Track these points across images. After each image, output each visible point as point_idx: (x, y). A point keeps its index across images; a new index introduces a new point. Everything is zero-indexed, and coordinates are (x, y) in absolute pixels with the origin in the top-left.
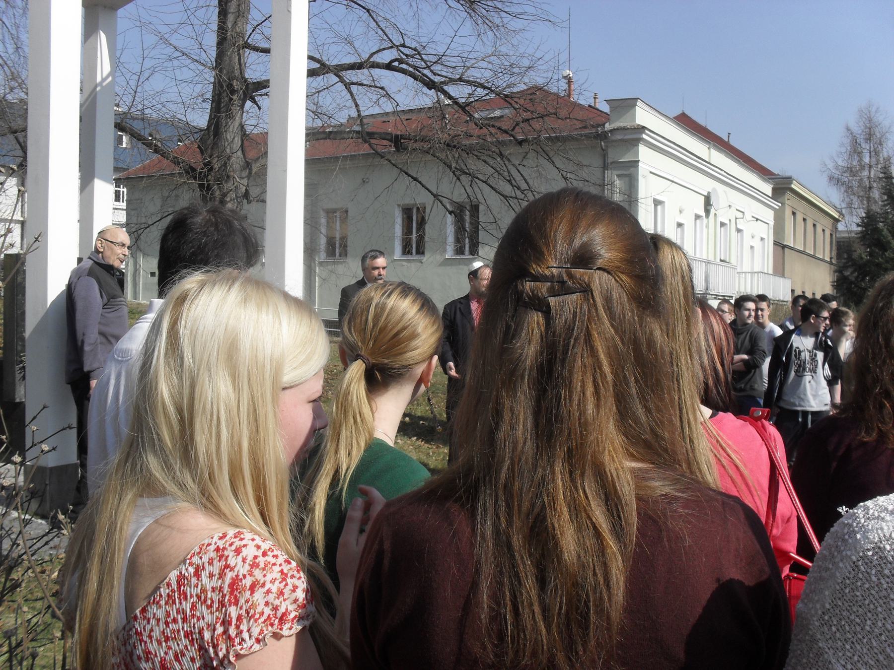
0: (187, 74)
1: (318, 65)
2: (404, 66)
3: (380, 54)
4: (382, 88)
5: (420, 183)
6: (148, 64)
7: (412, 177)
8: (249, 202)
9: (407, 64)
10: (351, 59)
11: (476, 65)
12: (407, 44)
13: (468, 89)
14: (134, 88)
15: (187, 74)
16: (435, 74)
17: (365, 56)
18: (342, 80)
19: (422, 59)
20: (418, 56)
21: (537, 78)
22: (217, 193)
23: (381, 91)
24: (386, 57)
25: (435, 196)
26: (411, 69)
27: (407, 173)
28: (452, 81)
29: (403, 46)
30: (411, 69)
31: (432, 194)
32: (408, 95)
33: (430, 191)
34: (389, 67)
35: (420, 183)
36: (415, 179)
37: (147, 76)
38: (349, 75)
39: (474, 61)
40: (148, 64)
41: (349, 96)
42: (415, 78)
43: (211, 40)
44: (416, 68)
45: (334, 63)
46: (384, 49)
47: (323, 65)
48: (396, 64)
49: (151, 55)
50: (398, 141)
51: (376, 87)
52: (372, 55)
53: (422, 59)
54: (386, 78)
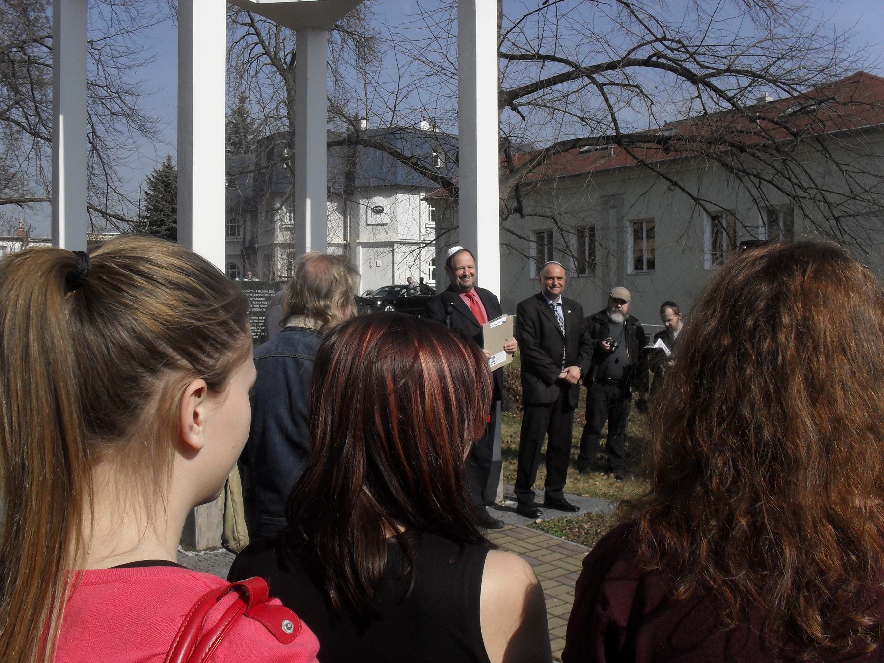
1: (571, 69)
3: (640, 51)
4: (637, 87)
6: (405, 82)
7: (671, 181)
8: (522, 217)
9: (665, 58)
10: (602, 59)
11: (747, 53)
12: (668, 37)
13: (745, 81)
16: (702, 67)
18: (594, 81)
20: (683, 49)
21: (819, 61)
24: (644, 54)
25: (696, 200)
26: (670, 63)
27: (664, 177)
28: (719, 73)
29: (665, 38)
30: (670, 63)
33: (690, 195)
34: (647, 63)
38: (599, 78)
40: (405, 82)
41: (601, 98)
44: (675, 61)
45: (584, 66)
47: (577, 67)
48: (654, 59)
51: (629, 85)
53: (687, 52)
54: (646, 77)
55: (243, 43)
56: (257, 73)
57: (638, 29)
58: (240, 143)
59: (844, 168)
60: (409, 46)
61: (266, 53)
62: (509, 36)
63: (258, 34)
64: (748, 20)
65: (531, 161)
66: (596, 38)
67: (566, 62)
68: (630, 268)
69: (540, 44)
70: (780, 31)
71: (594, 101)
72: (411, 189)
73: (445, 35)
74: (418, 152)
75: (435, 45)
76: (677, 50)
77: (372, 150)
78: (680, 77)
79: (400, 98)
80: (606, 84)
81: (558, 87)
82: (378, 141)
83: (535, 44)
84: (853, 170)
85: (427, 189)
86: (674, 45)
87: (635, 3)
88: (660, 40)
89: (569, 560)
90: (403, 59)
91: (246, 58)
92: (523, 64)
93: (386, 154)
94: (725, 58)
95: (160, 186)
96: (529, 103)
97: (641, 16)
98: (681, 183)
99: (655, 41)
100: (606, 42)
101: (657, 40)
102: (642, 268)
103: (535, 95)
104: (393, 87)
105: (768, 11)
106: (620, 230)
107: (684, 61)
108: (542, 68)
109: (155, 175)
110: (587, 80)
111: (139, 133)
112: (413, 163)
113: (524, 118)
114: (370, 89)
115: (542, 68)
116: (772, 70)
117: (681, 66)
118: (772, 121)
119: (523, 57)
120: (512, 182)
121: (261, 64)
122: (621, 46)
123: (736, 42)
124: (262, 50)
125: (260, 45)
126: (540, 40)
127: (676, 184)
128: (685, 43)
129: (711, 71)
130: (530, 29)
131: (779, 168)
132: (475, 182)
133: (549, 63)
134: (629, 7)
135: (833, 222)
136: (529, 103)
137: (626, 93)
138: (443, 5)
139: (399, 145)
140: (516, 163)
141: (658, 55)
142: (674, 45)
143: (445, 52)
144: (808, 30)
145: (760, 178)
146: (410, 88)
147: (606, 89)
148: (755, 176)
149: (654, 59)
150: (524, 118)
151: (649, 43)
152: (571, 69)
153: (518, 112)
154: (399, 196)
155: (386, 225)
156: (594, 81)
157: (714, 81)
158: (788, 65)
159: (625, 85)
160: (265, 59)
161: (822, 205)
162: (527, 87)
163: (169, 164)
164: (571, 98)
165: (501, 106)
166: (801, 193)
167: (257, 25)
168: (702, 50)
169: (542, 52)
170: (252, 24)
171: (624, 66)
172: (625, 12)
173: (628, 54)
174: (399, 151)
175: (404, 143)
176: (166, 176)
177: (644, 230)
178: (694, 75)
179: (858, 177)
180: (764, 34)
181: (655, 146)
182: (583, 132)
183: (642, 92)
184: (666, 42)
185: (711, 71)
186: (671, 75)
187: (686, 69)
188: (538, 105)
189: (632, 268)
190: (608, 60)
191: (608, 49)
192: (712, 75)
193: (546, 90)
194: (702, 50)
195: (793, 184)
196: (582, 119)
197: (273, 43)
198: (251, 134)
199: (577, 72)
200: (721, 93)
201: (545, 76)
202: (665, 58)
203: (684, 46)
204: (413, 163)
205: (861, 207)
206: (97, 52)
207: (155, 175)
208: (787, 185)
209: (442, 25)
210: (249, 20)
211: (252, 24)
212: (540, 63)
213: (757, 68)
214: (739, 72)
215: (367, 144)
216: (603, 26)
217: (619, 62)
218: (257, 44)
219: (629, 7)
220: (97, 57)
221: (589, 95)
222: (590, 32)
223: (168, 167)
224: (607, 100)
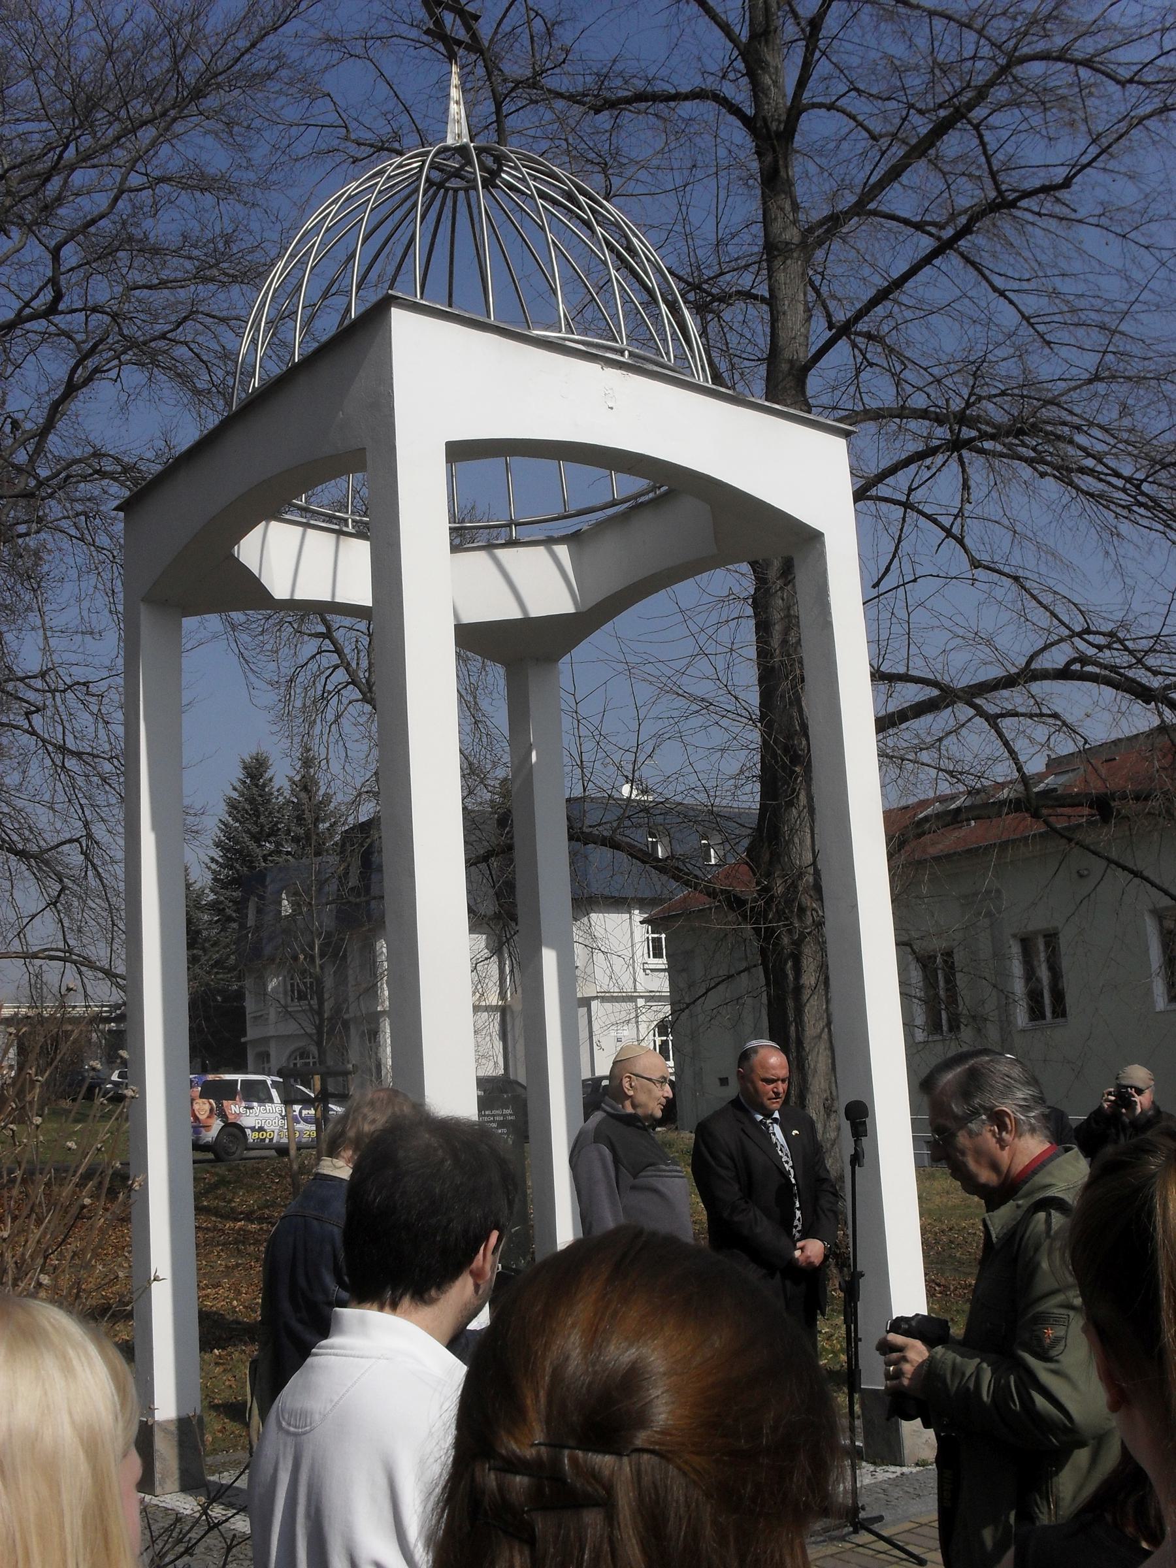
0: (718, 737)
1: (936, 692)
3: (1046, 654)
4: (1055, 716)
5: (1147, 879)
6: (649, 729)
7: (1131, 871)
10: (994, 672)
15: (718, 737)
16: (1156, 673)
17: (1022, 662)
18: (980, 712)
22: (786, 940)
23: (1051, 721)
24: (1057, 658)
26: (1104, 672)
27: (1118, 865)
29: (1088, 631)
30: (1104, 672)
32: (1105, 717)
34: (1064, 674)
35: (1147, 879)
36: (1136, 874)
40: (649, 729)
42: (1116, 686)
43: (747, 676)
44: (1113, 668)
46: (1052, 644)
48: (1077, 667)
49: (651, 715)
51: (1042, 715)
52: (1032, 658)
53: (1126, 649)
55: (313, 666)
56: (338, 717)
57: (1041, 617)
58: (308, 837)
61: (353, 682)
63: (338, 651)
67: (934, 684)
68: (1021, 1017)
72: (618, 903)
75: (703, 665)
76: (1109, 647)
80: (1002, 716)
85: (642, 903)
87: (1028, 574)
88: (1079, 635)
90: (645, 692)
91: (319, 693)
93: (622, 856)
101: (1074, 634)
102: (1044, 1017)
110: (967, 712)
114: (589, 745)
117: (1127, 678)
121: (345, 701)
124: (347, 678)
125: (341, 669)
133: (899, 686)
141: (1083, 660)
147: (1006, 724)
151: (1061, 640)
152: (936, 692)
154: (593, 916)
156: (980, 712)
159: (1036, 715)
160: (352, 693)
167: (338, 635)
170: (328, 635)
173: (1029, 663)
177: (1042, 947)
183: (1064, 724)
184: (1090, 638)
186: (1108, 692)
187: (1133, 681)
189: (1027, 1020)
193: (891, 731)
197: (365, 664)
198: (323, 821)
203: (1121, 641)
206: (93, 699)
210: (322, 629)
211: (328, 635)
216: (991, 620)
217: (1018, 674)
218: (336, 667)
220: (95, 709)
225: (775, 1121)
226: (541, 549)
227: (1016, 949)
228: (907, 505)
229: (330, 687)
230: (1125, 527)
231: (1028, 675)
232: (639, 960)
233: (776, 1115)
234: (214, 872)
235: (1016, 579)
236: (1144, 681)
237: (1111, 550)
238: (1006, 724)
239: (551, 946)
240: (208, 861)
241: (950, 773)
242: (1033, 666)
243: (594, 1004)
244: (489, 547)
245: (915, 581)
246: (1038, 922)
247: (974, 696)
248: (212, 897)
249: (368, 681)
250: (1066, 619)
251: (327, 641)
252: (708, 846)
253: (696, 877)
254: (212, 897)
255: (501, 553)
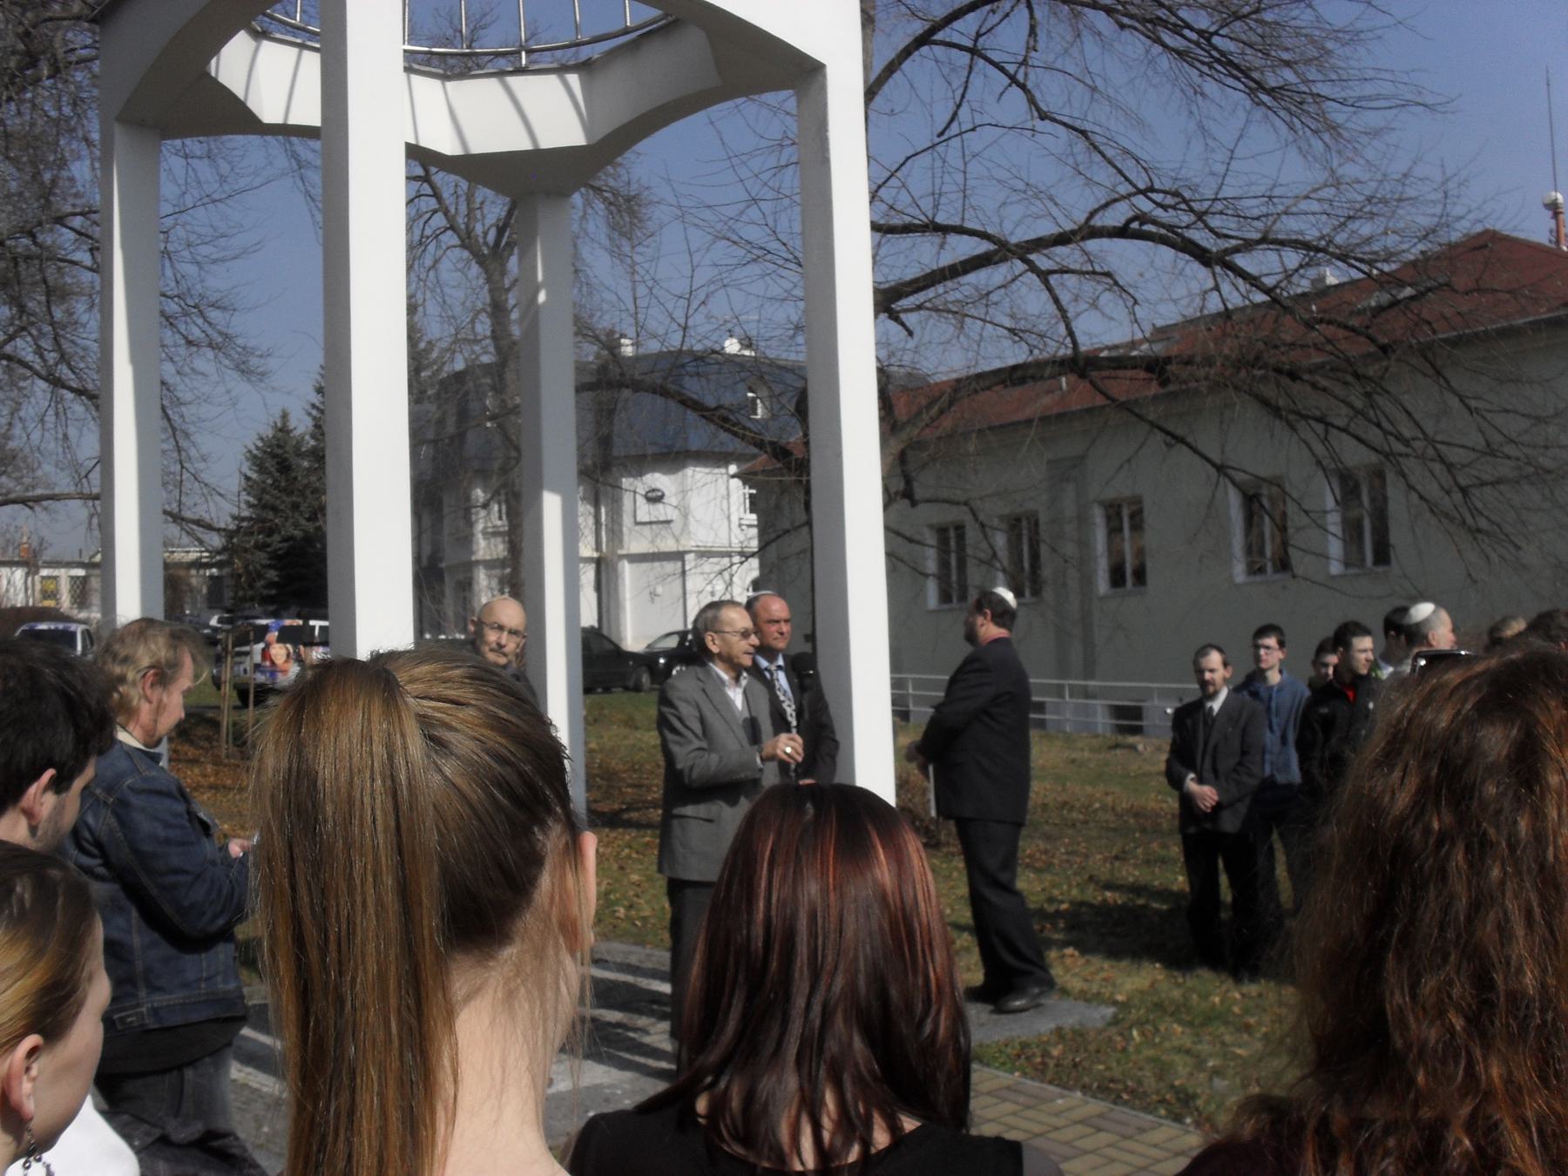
1: (992, 247)
2: (1147, 227)
4: (1108, 274)
8: (914, 504)
9: (1155, 222)
10: (1046, 229)
11: (1294, 209)
12: (1157, 186)
13: (1292, 258)
14: (682, 321)
17: (1081, 217)
18: (1033, 268)
19: (1192, 210)
20: (1183, 206)
24: (1116, 216)
25: (1221, 469)
26: (1163, 231)
27: (1162, 429)
28: (1248, 246)
29: (1151, 189)
30: (1163, 231)
31: (1214, 465)
34: (1123, 232)
37: (702, 297)
38: (1041, 261)
39: (1290, 202)
41: (1045, 295)
44: (1170, 228)
45: (1014, 240)
48: (1135, 225)
50: (1155, 367)
51: (1094, 273)
52: (1092, 214)
53: (1192, 210)
56: (436, 262)
57: (1104, 175)
59: (1473, 404)
60: (707, 215)
61: (452, 228)
62: (882, 193)
63: (436, 195)
64: (1293, 152)
65: (929, 406)
66: (1032, 192)
68: (1102, 585)
69: (936, 206)
70: (1349, 171)
71: (1032, 300)
72: (714, 457)
73: (770, 195)
74: (728, 399)
75: (754, 213)
76: (1174, 208)
77: (647, 399)
78: (1181, 255)
79: (694, 305)
81: (971, 278)
82: (659, 381)
83: (926, 205)
84: (1488, 407)
86: (1170, 200)
87: (1097, 129)
88: (1143, 192)
89: (1030, 1113)
90: (698, 238)
92: (906, 241)
93: (672, 404)
94: (1258, 219)
95: (270, 464)
96: (919, 307)
97: (1110, 153)
98: (1189, 439)
99: (1134, 194)
100: (1051, 199)
103: (931, 293)
104: (681, 287)
105: (1326, 137)
106: (1083, 520)
107: (1188, 227)
108: (942, 246)
109: (260, 444)
110: (1020, 266)
111: (236, 375)
112: (722, 418)
113: (910, 333)
114: (642, 290)
115: (942, 246)
116: (1340, 239)
117: (1183, 238)
118: (1346, 327)
119: (907, 229)
120: (896, 446)
122: (1075, 206)
123: (1277, 192)
125: (440, 215)
126: (937, 196)
127: (1181, 440)
128: (1187, 194)
129: (1234, 242)
130: (919, 178)
131: (1359, 404)
132: (838, 455)
133: (953, 239)
134: (1087, 138)
135: (1458, 497)
136: (919, 307)
137: (1089, 287)
138: (764, 143)
139: (693, 387)
140: (901, 412)
141: (1142, 218)
142: (1170, 200)
143: (771, 224)
144: (1397, 168)
145: (1328, 425)
146: (712, 288)
147: (1053, 279)
148: (1319, 420)
149: (1135, 225)
150: (910, 333)
151: (1123, 198)
152: (992, 247)
153: (903, 324)
154: (689, 471)
155: (668, 522)
156: (1033, 268)
157: (1241, 260)
158: (1366, 229)
160: (450, 238)
161: (1437, 467)
162: (916, 281)
163: (284, 425)
164: (994, 297)
165: (876, 316)
166: (1398, 447)
168: (1219, 206)
169: (939, 220)
170: (426, 179)
171: (1083, 239)
172: (1081, 145)
174: (695, 397)
175: (704, 382)
176: (279, 446)
177: (1125, 516)
178: (1205, 251)
179: (1499, 420)
180: (1321, 176)
181: (1142, 374)
182: (1015, 355)
183: (1116, 283)
184: (1153, 196)
185: (1234, 242)
186: (1167, 253)
188: (937, 310)
190: (1055, 230)
191: (1055, 211)
192: (1236, 250)
193: (949, 284)
194: (1219, 206)
195: (1386, 433)
196: (1011, 331)
197: (463, 209)
198: (426, 368)
199: (1001, 251)
200: (1253, 281)
201: (947, 259)
202: (1155, 222)
203: (1185, 201)
204: (722, 418)
205: (1505, 469)
207: (260, 444)
208: (1374, 435)
209: (765, 177)
211: (426, 179)
212: (936, 239)
213: (1311, 235)
214: (1282, 243)
215: (636, 386)
217: (1073, 232)
218: (435, 212)
219: (1087, 138)
221: (1024, 290)
222: (1022, 179)
223: (283, 429)
224: (1056, 301)
225: (779, 667)
226: (553, 79)
227: (1098, 516)
228: (973, 51)
229: (428, 232)
230: (1210, 87)
231: (1090, 231)
232: (734, 519)
233: (781, 662)
234: (314, 418)
235: (1083, 133)
236: (1204, 244)
237: (1194, 108)
238: (1053, 279)
239: (554, 490)
240: (308, 407)
241: (1010, 330)
242: (1092, 223)
243: (689, 557)
244: (501, 74)
245: (973, 130)
246: (1120, 488)
247: (1030, 251)
248: (313, 443)
249: (467, 225)
250: (1132, 177)
251: (426, 185)
252: (754, 400)
253: (744, 428)
254: (313, 443)
255: (513, 81)
